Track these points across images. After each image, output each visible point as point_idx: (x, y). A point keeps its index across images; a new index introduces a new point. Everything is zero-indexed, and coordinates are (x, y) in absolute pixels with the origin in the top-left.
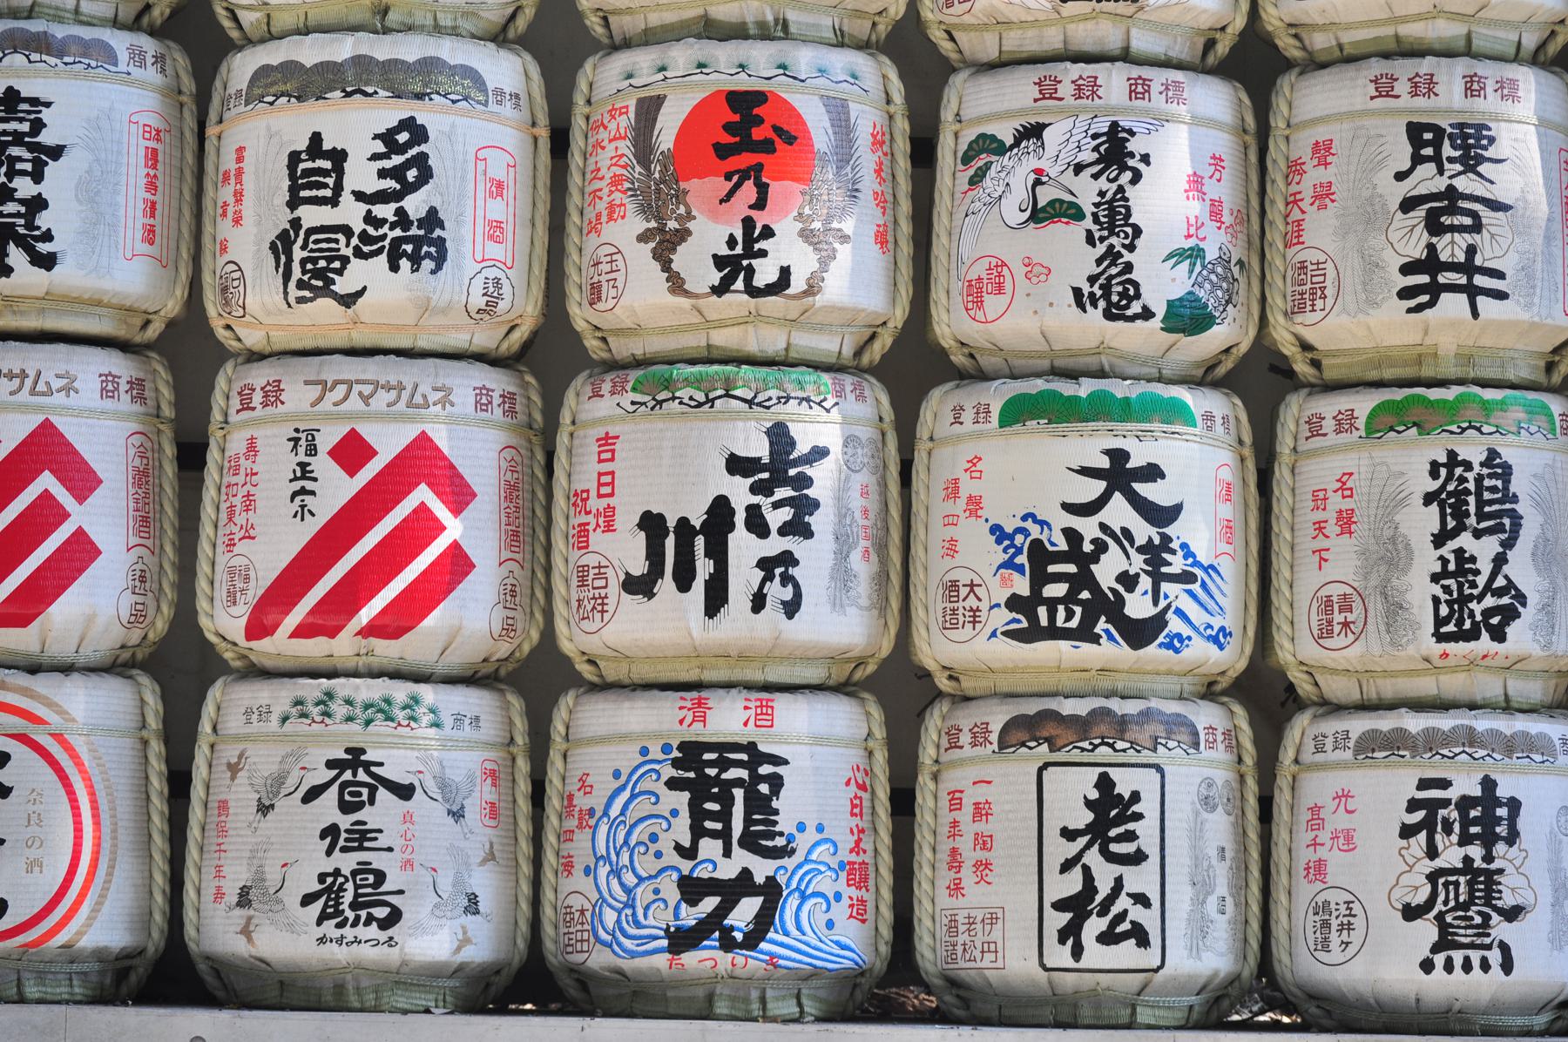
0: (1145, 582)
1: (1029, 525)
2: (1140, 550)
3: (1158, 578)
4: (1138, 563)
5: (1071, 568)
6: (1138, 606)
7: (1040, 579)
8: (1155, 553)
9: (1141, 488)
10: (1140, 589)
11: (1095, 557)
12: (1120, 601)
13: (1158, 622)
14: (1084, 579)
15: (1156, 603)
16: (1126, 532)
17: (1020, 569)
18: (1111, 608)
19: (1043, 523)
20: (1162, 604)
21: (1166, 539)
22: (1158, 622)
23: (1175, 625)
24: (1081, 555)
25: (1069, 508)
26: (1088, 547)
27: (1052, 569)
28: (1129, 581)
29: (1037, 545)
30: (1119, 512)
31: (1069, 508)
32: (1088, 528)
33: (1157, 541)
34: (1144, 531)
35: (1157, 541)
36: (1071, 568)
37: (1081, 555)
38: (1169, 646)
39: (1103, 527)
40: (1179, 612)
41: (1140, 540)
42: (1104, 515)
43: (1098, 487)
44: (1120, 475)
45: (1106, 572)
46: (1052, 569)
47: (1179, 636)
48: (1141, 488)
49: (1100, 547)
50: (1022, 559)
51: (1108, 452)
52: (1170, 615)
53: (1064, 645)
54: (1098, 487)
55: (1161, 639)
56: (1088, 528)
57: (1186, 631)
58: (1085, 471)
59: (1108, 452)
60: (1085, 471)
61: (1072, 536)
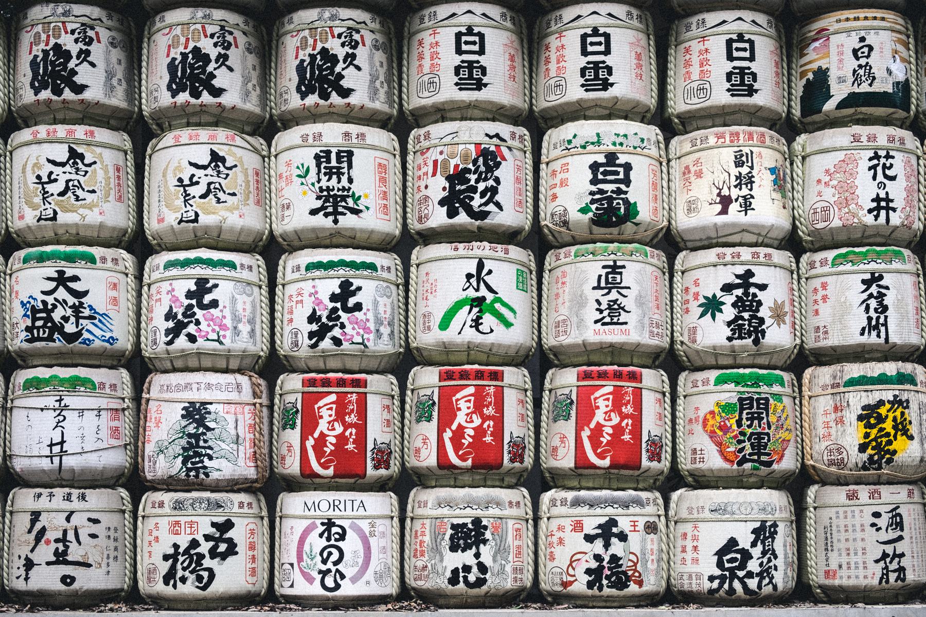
0: (73, 319)
1: (31, 300)
2: (70, 307)
3: (78, 318)
4: (69, 312)
5: (44, 315)
6: (70, 328)
7: (35, 319)
8: (77, 309)
9: (70, 284)
10: (70, 322)
11: (52, 310)
12: (63, 327)
13: (78, 334)
14: (49, 319)
15: (77, 327)
16: (64, 301)
17: (28, 316)
18: (60, 329)
19: (35, 299)
20: (80, 327)
21: (81, 304)
22: (78, 334)
23: (86, 335)
24: (48, 310)
25: (43, 293)
26: (50, 307)
27: (38, 315)
28: (66, 319)
29: (33, 306)
30: (62, 293)
31: (43, 293)
32: (50, 300)
33: (77, 304)
34: (71, 300)
35: (77, 304)
36: (44, 315)
37: (48, 310)
38: (84, 343)
39: (56, 299)
40: (88, 331)
41: (70, 304)
42: (55, 295)
43: (55, 284)
44: (61, 280)
45: (57, 316)
46: (38, 315)
47: (89, 340)
48: (70, 284)
49: (55, 306)
50: (29, 313)
51: (57, 271)
52: (84, 331)
53: (43, 344)
54: (55, 284)
55: (80, 340)
56: (50, 300)
57: (91, 337)
58: (49, 279)
59: (57, 271)
60: (49, 279)
61: (44, 303)
